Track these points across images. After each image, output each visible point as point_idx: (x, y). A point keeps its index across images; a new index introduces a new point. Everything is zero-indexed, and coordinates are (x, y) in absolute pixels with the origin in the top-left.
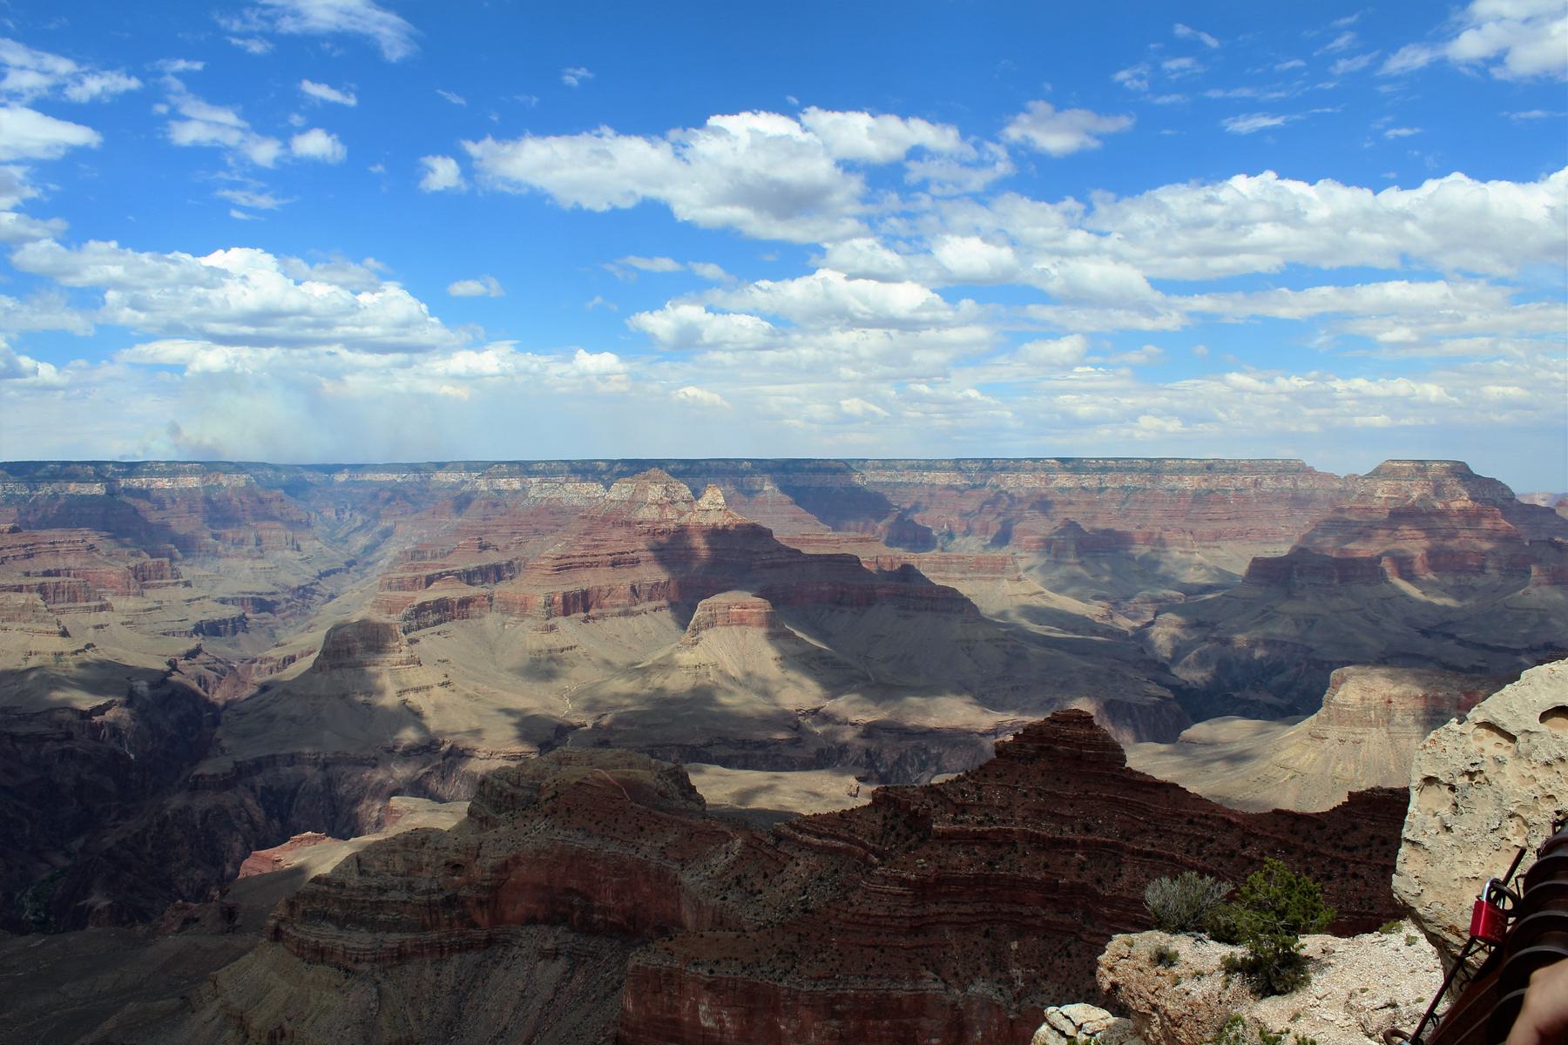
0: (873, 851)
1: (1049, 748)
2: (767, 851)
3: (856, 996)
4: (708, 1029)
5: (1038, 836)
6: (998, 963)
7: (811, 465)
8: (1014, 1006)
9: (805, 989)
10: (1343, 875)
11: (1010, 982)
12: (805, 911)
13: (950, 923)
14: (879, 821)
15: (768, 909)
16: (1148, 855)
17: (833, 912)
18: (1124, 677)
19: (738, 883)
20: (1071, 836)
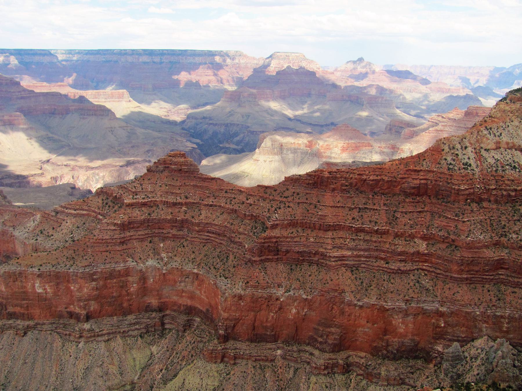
0: (99, 214)
1: (168, 167)
3: (101, 271)
4: (39, 293)
5: (167, 202)
6: (156, 253)
7: (32, 52)
8: (165, 268)
9: (80, 271)
10: (284, 207)
11: (162, 259)
12: (74, 241)
13: (136, 239)
14: (101, 201)
15: (57, 242)
16: (211, 206)
17: (88, 240)
18: (177, 140)
19: (42, 233)
20: (180, 201)
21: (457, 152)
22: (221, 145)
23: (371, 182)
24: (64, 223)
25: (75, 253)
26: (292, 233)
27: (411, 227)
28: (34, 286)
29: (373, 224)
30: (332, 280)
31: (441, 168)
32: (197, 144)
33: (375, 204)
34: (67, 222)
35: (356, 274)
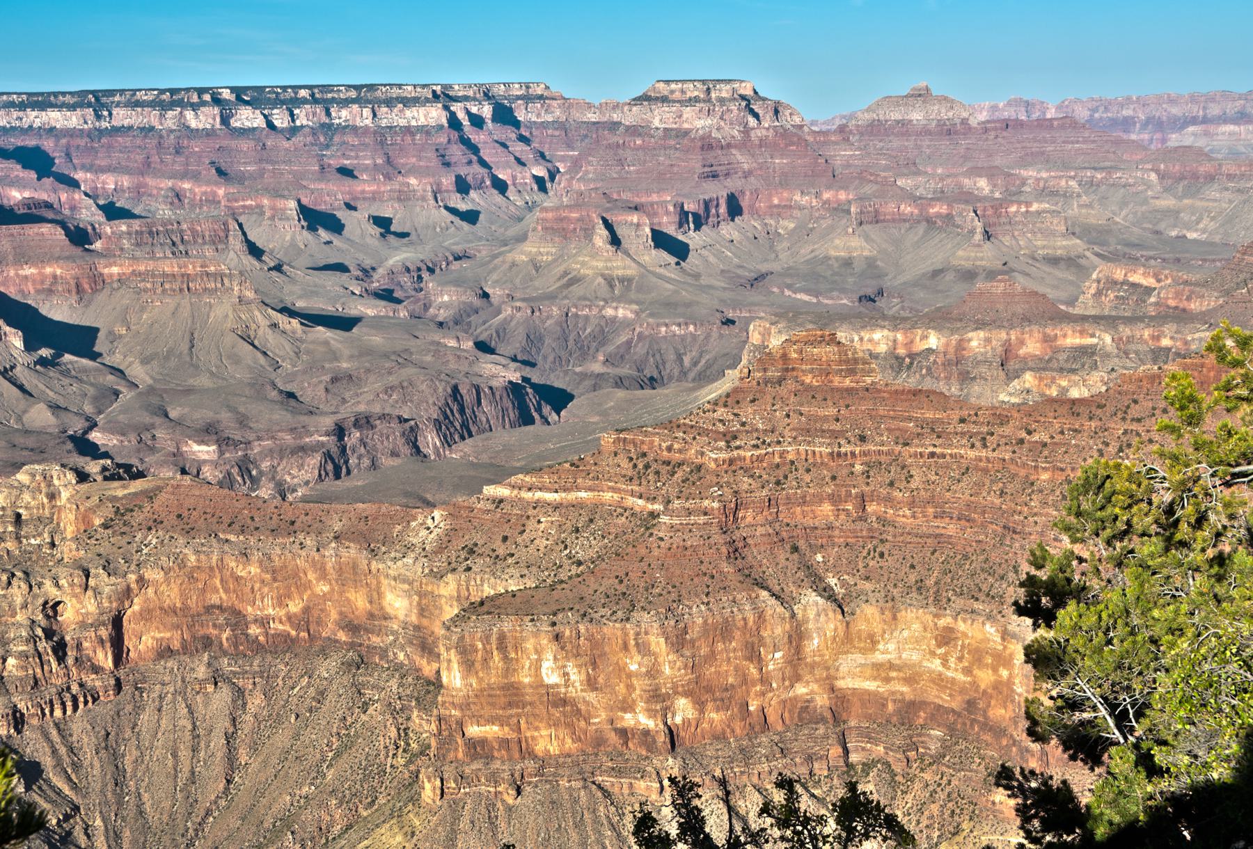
24: (531, 524)
34: (539, 522)
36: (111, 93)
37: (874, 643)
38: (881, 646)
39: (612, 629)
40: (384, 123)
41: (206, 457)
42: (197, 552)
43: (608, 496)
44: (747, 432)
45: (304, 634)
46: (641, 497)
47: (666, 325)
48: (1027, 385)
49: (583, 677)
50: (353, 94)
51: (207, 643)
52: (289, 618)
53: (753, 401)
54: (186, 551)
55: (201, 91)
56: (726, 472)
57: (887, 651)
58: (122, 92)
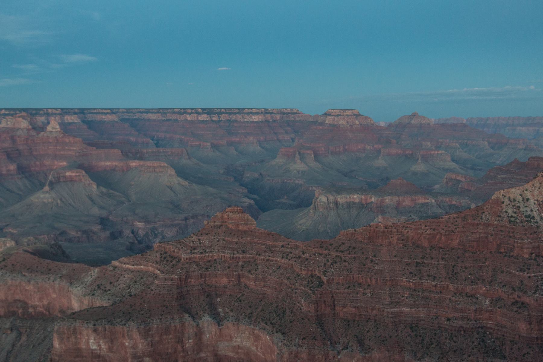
2: (109, 273)
4: (93, 350)
12: (131, 296)
14: (159, 256)
15: (114, 297)
16: (268, 260)
19: (99, 287)
21: (518, 205)
22: (278, 201)
23: (428, 236)
25: (131, 307)
26: (349, 287)
27: (472, 282)
28: (88, 343)
29: (431, 278)
30: (391, 337)
31: (502, 220)
32: (255, 200)
33: (432, 258)
34: (124, 277)
35: (416, 331)
36: (167, 109)
37: (231, 338)
38: (234, 339)
39: (119, 328)
40: (246, 120)
41: (141, 227)
42: (12, 279)
43: (150, 269)
44: (201, 247)
45: (47, 313)
46: (159, 270)
47: (312, 187)
48: (380, 220)
49: (107, 347)
50: (238, 111)
51: (14, 314)
52: (43, 306)
53: (207, 234)
54: (8, 279)
55: (192, 109)
56: (187, 263)
57: (237, 341)
58: (170, 109)
